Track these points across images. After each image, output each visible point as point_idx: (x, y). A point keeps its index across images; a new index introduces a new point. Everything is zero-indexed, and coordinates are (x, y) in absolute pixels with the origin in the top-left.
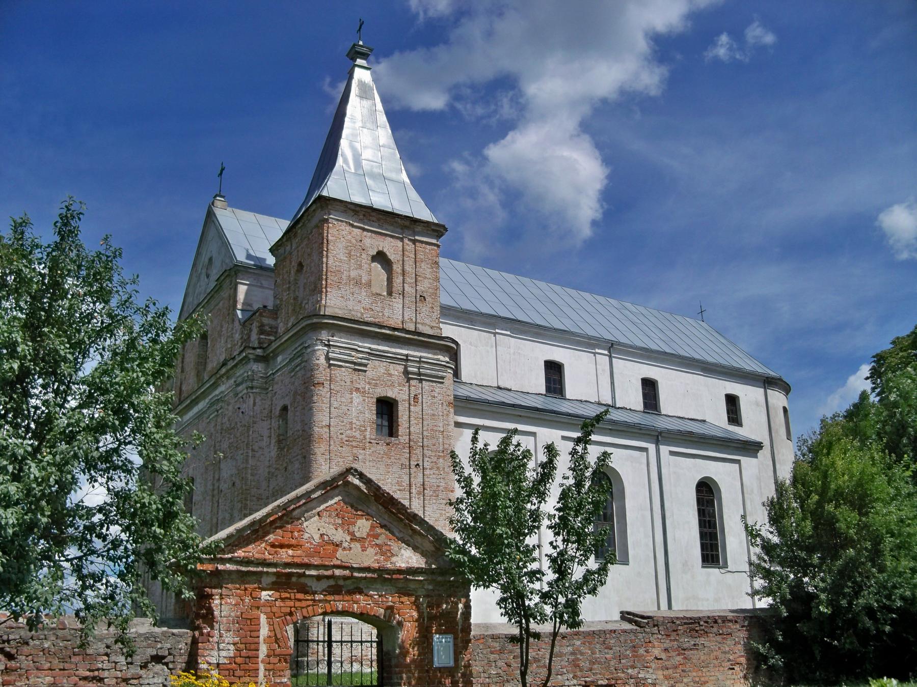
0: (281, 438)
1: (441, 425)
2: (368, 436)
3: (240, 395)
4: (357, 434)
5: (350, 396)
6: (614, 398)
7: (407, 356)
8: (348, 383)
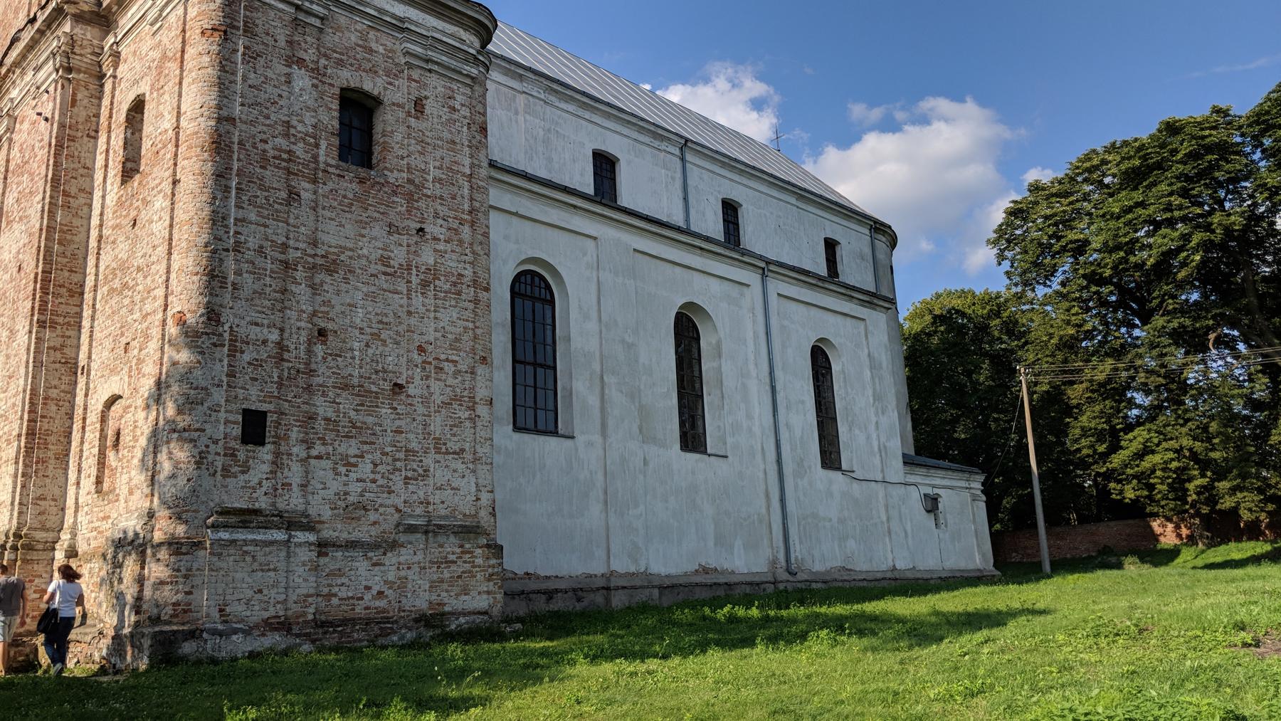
0: (129, 165)
1: (467, 162)
2: (322, 159)
3: (43, 88)
4: (299, 149)
5: (287, 70)
6: (687, 220)
7: (401, 20)
8: (282, 43)
